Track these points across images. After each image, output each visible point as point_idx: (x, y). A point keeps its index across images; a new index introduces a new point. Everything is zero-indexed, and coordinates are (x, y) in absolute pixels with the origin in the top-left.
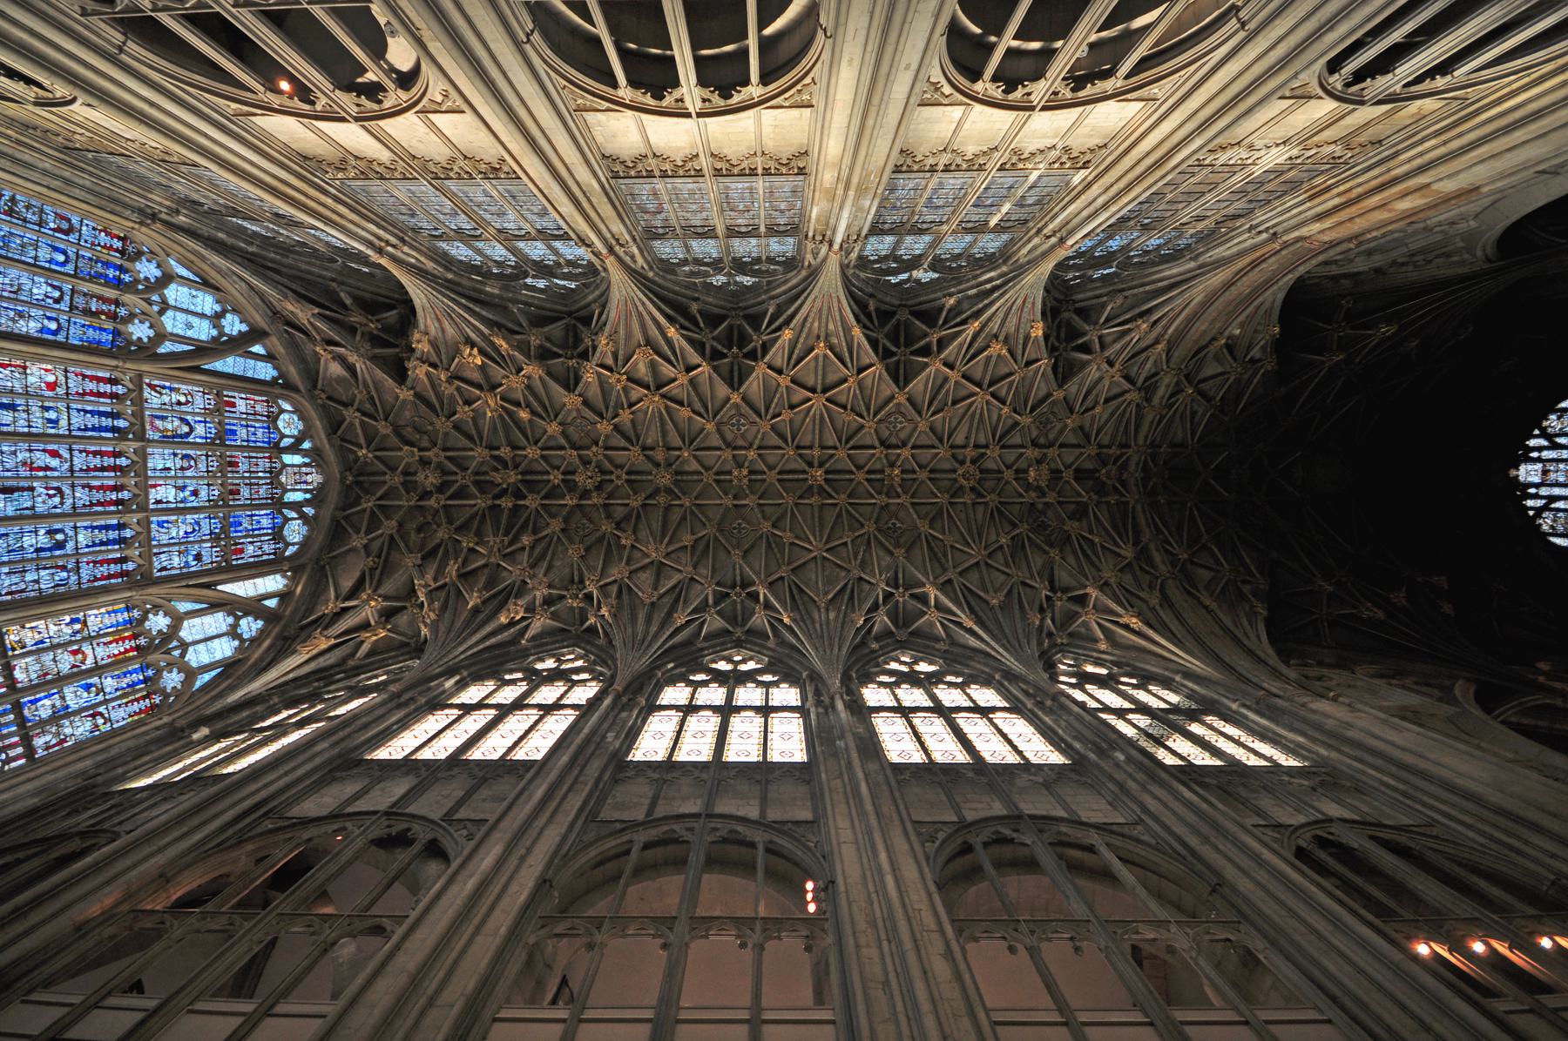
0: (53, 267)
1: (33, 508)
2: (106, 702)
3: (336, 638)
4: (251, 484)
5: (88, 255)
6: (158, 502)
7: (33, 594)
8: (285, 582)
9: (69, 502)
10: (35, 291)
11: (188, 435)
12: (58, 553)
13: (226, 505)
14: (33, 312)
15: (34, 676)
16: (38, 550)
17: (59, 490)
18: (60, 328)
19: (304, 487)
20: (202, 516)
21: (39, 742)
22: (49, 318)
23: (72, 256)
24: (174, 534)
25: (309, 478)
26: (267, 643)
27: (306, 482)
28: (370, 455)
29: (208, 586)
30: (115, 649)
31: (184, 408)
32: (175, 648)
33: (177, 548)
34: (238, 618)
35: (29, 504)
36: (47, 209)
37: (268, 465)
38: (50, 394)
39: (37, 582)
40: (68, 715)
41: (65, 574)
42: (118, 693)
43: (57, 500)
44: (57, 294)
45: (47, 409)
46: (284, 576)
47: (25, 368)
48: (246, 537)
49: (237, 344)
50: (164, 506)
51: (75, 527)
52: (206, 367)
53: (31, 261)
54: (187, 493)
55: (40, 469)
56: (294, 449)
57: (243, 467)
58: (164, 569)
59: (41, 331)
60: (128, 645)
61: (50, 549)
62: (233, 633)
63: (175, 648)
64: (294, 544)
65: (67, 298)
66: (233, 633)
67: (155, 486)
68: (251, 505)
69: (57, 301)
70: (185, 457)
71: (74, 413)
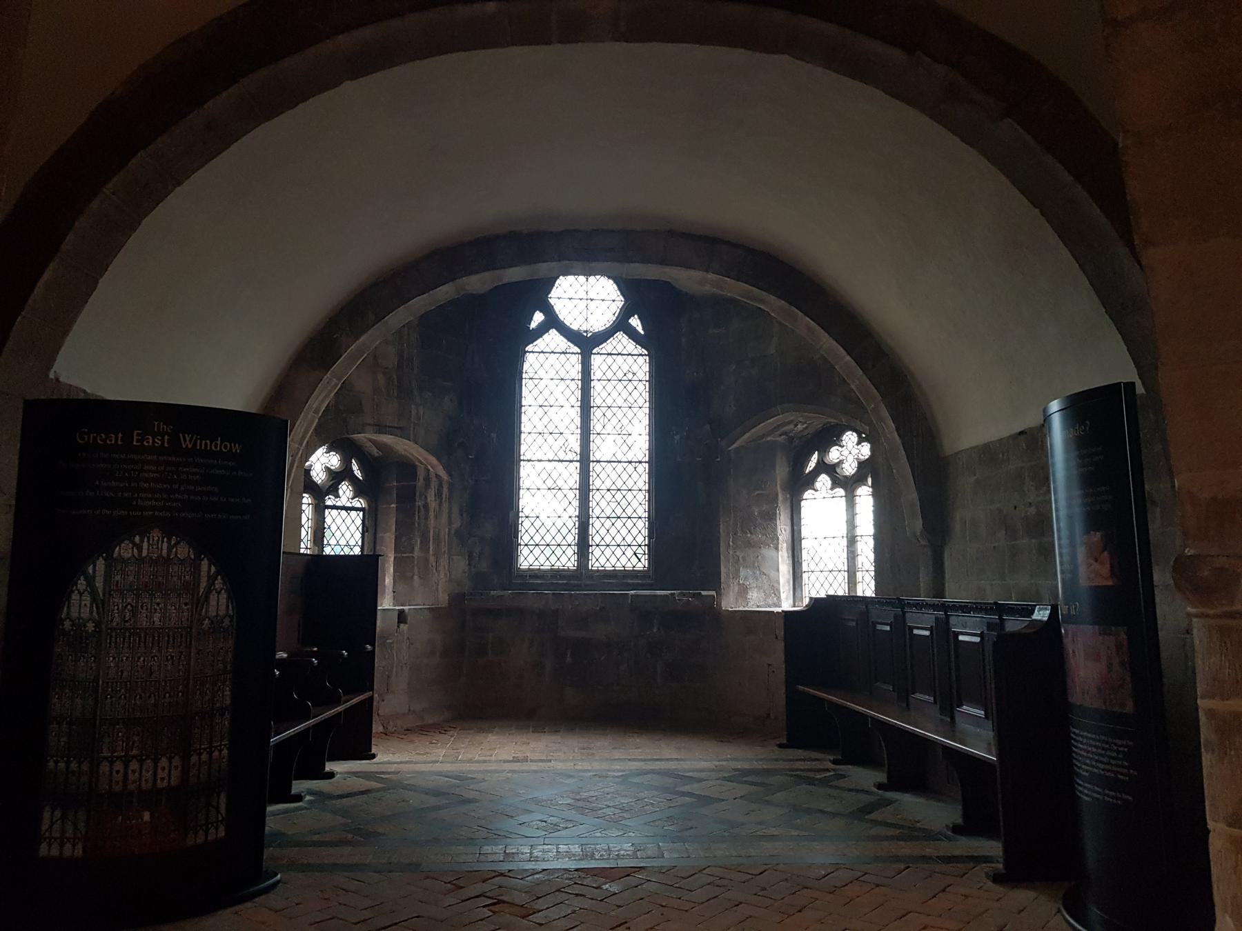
8: (206, 559)
11: (132, 606)
19: (160, 542)
27: (159, 540)
46: (202, 560)
49: (90, 581)
56: (140, 548)
64: (189, 552)
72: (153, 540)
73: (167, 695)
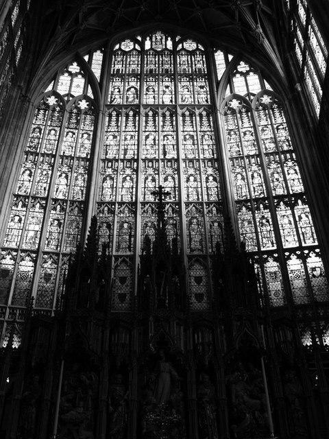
0: (58, 134)
1: (173, 145)
2: (272, 124)
3: (257, 24)
4: (162, 64)
5: (49, 122)
6: (171, 101)
7: (214, 147)
9: (171, 133)
10: (70, 140)
11: (135, 88)
12: (195, 138)
13: (174, 75)
14: (80, 141)
15: (254, 148)
16: (194, 144)
17: (164, 136)
18: (86, 133)
19: (164, 40)
20: (179, 84)
21: (286, 148)
22: (82, 136)
23: (51, 128)
24: (189, 96)
25: (159, 38)
26: (254, 60)
27: (161, 39)
28: (144, 4)
29: (218, 83)
30: (246, 120)
31: (122, 90)
32: (249, 98)
33: (196, 96)
34: (238, 72)
35: (172, 147)
36: (31, 136)
37: (151, 56)
38: (118, 137)
39: (209, 145)
40: (275, 138)
41: (206, 136)
42: (269, 120)
43: (169, 137)
44: (71, 134)
45: (126, 139)
47: (107, 145)
48: (192, 67)
50: (173, 99)
51: (183, 131)
52: (99, 80)
53: (56, 142)
54: (167, 90)
55: (155, 142)
56: (142, 44)
57: (153, 67)
58: (207, 101)
59: (89, 140)
60: (244, 115)
61: (194, 140)
62: (245, 75)
63: (249, 98)
65: (72, 130)
66: (245, 75)
67: (163, 102)
68: (174, 64)
69: (74, 134)
70: (147, 90)
71: (127, 130)
72: (156, 39)
73: (192, 178)
